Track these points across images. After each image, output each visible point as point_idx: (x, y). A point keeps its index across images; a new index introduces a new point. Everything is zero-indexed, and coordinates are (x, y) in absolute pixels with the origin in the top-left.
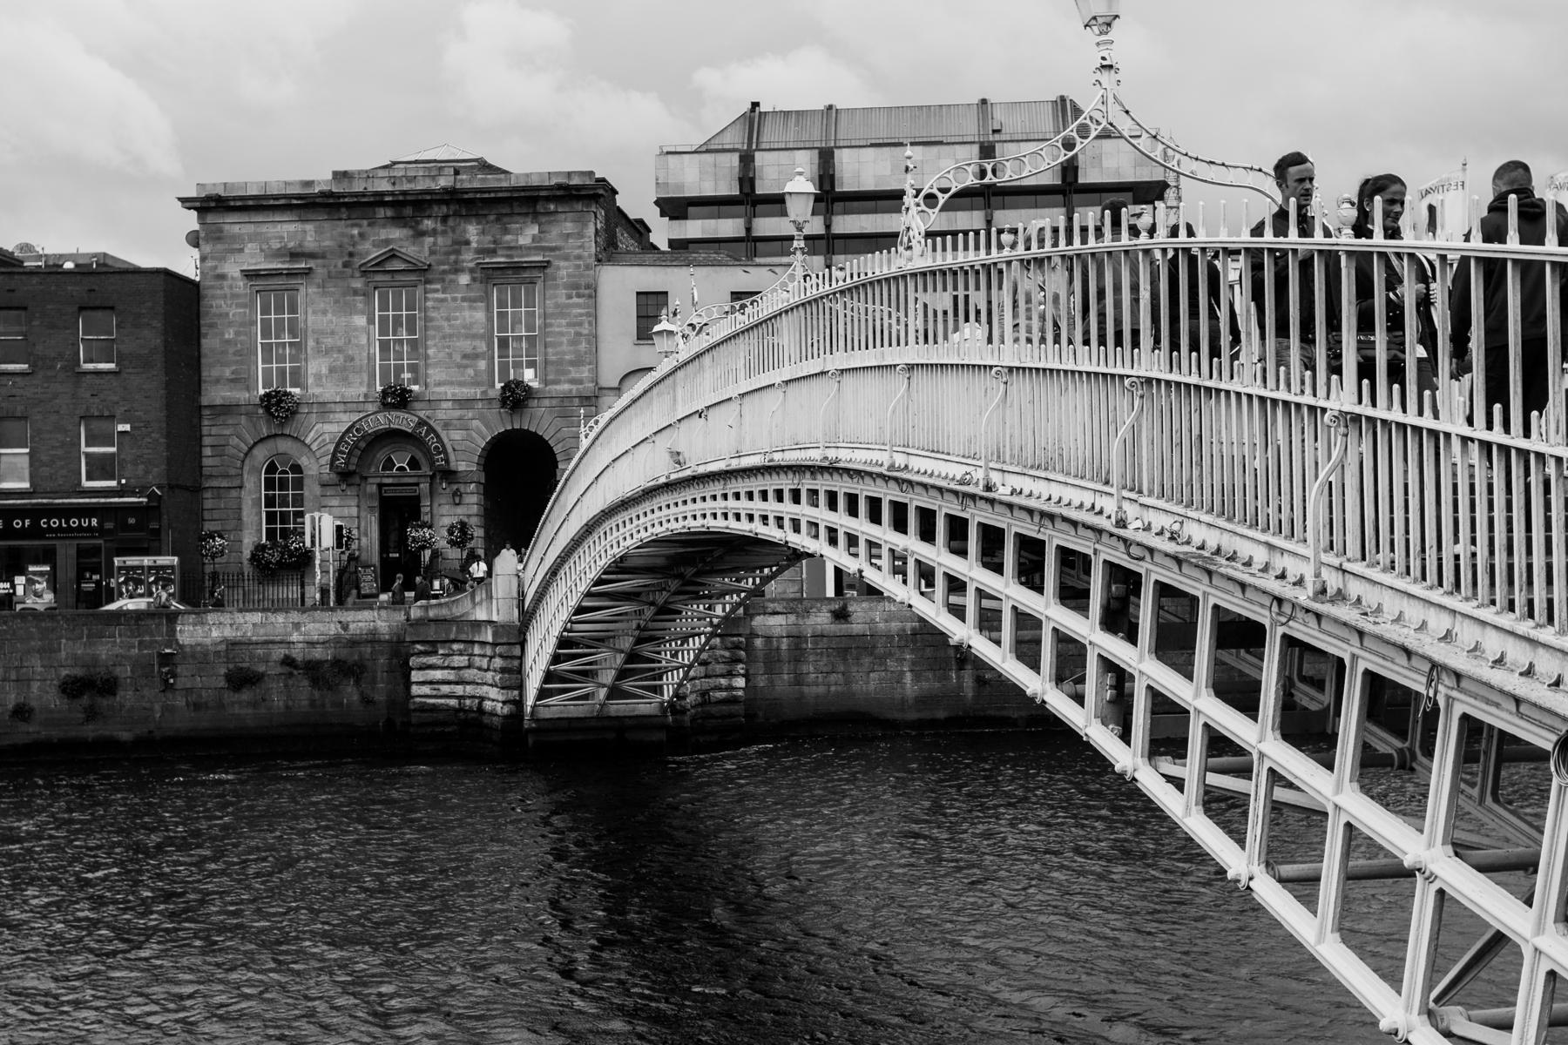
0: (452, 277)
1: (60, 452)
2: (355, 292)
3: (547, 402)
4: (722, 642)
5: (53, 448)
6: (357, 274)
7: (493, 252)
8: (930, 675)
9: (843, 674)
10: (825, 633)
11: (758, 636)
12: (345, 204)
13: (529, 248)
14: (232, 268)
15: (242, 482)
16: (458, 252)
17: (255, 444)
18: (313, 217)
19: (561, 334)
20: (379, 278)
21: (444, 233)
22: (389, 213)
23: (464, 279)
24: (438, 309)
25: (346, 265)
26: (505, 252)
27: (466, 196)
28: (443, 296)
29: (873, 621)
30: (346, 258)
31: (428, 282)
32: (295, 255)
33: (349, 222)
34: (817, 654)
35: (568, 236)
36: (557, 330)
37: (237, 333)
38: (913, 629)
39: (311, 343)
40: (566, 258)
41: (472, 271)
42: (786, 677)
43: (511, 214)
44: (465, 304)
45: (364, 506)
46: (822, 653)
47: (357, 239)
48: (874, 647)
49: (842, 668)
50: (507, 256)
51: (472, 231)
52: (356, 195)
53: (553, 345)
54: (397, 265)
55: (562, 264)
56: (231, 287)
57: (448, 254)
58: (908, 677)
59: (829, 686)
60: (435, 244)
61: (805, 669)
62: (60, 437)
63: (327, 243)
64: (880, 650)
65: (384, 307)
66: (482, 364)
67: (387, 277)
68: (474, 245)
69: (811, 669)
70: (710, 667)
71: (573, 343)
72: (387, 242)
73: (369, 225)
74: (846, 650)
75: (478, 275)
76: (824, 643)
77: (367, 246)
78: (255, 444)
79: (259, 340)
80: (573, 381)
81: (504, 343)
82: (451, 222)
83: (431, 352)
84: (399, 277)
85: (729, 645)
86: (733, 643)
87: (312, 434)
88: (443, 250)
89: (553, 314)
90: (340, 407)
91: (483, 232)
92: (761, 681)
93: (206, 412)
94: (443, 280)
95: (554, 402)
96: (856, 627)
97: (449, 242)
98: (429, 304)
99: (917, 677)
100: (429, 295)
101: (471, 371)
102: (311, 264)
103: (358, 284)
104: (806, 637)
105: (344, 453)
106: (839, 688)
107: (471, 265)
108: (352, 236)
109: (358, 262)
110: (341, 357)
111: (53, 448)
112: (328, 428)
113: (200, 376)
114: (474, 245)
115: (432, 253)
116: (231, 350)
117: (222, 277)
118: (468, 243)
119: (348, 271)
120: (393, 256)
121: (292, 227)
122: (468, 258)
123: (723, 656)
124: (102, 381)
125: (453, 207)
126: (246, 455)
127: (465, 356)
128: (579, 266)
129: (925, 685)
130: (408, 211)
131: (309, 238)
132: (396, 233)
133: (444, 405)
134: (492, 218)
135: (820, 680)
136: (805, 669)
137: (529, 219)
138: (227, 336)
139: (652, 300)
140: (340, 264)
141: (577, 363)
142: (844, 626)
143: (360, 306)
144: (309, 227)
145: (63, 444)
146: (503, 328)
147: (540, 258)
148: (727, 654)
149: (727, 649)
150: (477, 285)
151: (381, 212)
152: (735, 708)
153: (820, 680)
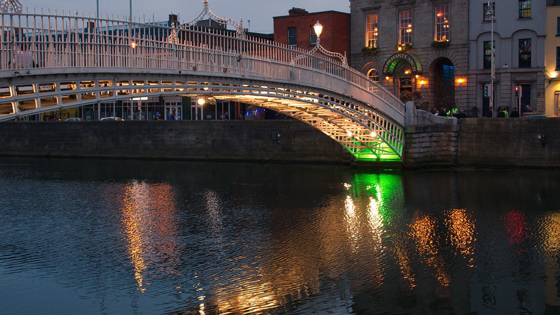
0: (422, 4)
3: (451, 47)
14: (358, 9)
20: (400, 7)
67: (403, 7)
86: (449, 134)
93: (352, 56)
100: (415, 12)
103: (394, 9)
105: (386, 68)
117: (356, 11)
133: (419, 50)
140: (389, 3)
148: (446, 138)
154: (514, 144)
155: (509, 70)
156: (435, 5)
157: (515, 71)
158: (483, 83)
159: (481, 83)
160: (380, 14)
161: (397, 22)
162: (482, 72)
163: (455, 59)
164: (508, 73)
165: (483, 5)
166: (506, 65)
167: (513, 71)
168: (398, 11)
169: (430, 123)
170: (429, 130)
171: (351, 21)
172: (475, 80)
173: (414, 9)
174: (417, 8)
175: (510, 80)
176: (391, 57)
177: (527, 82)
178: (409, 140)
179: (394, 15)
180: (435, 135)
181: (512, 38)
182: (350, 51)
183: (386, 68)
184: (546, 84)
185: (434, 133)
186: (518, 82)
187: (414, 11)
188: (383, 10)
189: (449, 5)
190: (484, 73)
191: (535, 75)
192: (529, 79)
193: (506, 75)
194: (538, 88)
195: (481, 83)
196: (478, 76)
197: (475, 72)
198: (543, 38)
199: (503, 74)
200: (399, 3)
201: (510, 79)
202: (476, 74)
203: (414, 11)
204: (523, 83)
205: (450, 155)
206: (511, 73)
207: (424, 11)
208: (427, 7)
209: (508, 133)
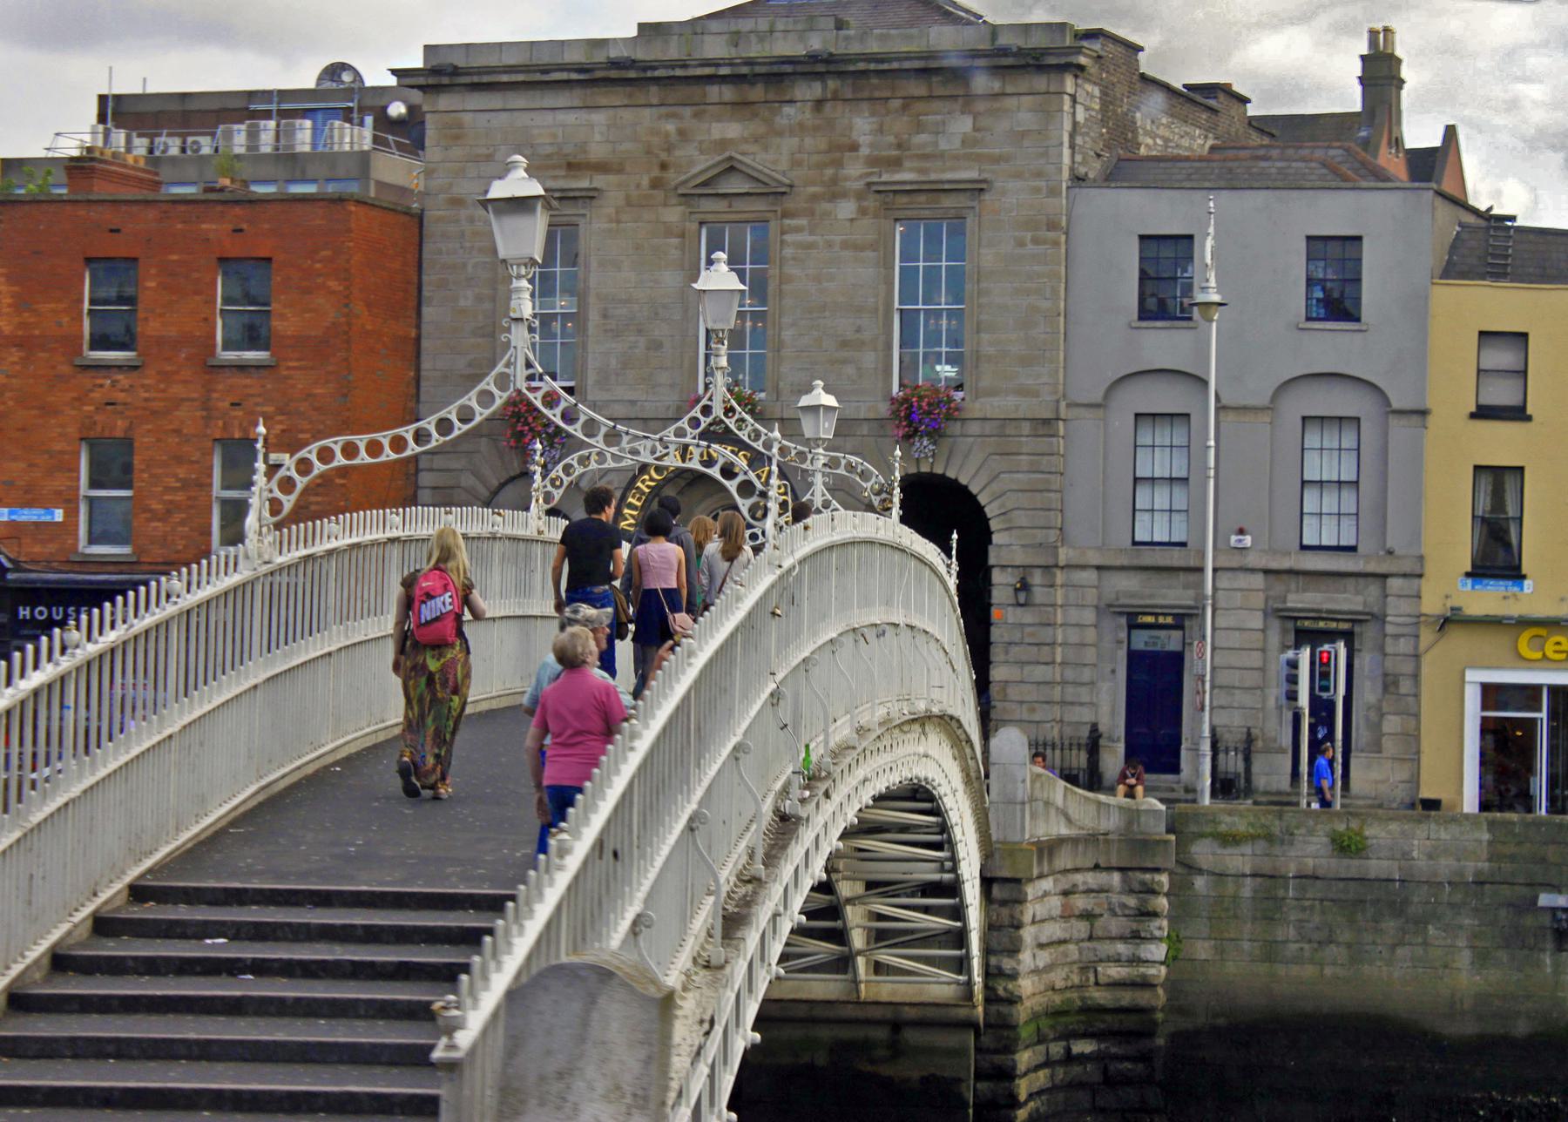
0: (826, 206)
1: (179, 497)
2: (669, 233)
3: (974, 428)
4: (1124, 881)
5: (168, 490)
6: (674, 201)
7: (896, 163)
8: (1503, 955)
9: (1349, 946)
10: (1320, 873)
11: (1200, 871)
12: (656, 80)
13: (956, 158)
16: (838, 164)
17: (503, 485)
18: (604, 101)
20: (708, 205)
21: (816, 129)
22: (728, 93)
23: (846, 209)
25: (656, 184)
26: (916, 164)
27: (852, 68)
29: (1406, 856)
30: (656, 173)
31: (785, 215)
32: (570, 166)
33: (663, 110)
34: (1304, 909)
35: (1024, 134)
37: (479, 299)
38: (1478, 873)
39: (594, 316)
40: (1018, 175)
41: (860, 196)
42: (1246, 945)
43: (931, 97)
44: (847, 254)
46: (1312, 908)
47: (674, 137)
48: (1406, 902)
49: (1346, 936)
50: (921, 171)
51: (862, 126)
52: (672, 65)
54: (735, 185)
55: (1011, 185)
57: (821, 166)
58: (1464, 959)
59: (1322, 965)
60: (800, 150)
61: (1280, 933)
62: (182, 472)
63: (627, 146)
64: (1412, 910)
66: (869, 359)
67: (721, 205)
68: (865, 151)
69: (1292, 932)
70: (1099, 923)
72: (723, 144)
73: (696, 115)
74: (1360, 902)
75: (871, 202)
76: (1315, 890)
77: (690, 151)
78: (503, 485)
80: (1023, 392)
81: (908, 318)
82: (828, 106)
83: (787, 335)
84: (739, 205)
85: (1136, 887)
86: (1143, 883)
88: (815, 158)
91: (881, 130)
92: (1202, 950)
94: (812, 213)
95: (988, 428)
96: (1376, 867)
97: (823, 146)
98: (788, 252)
99: (1482, 959)
100: (788, 238)
101: (850, 370)
102: (599, 181)
103: (673, 215)
104: (1285, 878)
105: (634, 508)
106: (1340, 971)
107: (859, 185)
108: (667, 135)
109: (673, 177)
111: (168, 490)
113: (418, 370)
114: (865, 151)
115: (796, 163)
118: (854, 147)
119: (659, 194)
120: (731, 169)
121: (570, 118)
122: (854, 171)
123: (1124, 906)
124: (248, 381)
125: (832, 84)
127: (844, 344)
128: (1037, 190)
129: (1494, 975)
130: (757, 93)
131: (598, 137)
132: (732, 130)
134: (896, 104)
135: (1307, 954)
136: (1280, 933)
137: (957, 106)
138: (462, 303)
139: (1167, 251)
140: (645, 182)
141: (1026, 361)
142: (1356, 862)
143: (675, 254)
144: (599, 118)
145: (186, 485)
146: (908, 295)
147: (973, 175)
148: (1132, 901)
149: (1132, 891)
150: (866, 222)
151: (713, 92)
152: (1142, 998)
153: (1307, 954)
154: (1431, 930)
155: (1253, 560)
157: (1286, 564)
158: (1129, 614)
159: (1121, 614)
162: (1125, 562)
164: (1253, 570)
166: (1241, 532)
167: (1274, 565)
168: (695, 226)
169: (1064, 831)
170: (1064, 860)
171: (428, 248)
172: (1091, 596)
173: (787, 222)
174: (803, 222)
175: (1262, 606)
177: (1337, 620)
178: (1005, 912)
180: (1085, 883)
181: (1270, 408)
182: (418, 401)
184: (1427, 636)
185: (1079, 878)
186: (1296, 619)
188: (611, 211)
190: (1136, 562)
191: (1373, 589)
192: (1345, 607)
193: (1243, 581)
194: (1389, 649)
195: (1121, 614)
196: (1106, 575)
197: (1094, 558)
198: (1415, 419)
199: (1229, 574)
200: (705, 184)
201: (1258, 600)
202: (1099, 568)
204: (1322, 624)
205: (1145, 984)
206: (1267, 572)
207: (838, 239)
208: (852, 220)
209: (1402, 881)
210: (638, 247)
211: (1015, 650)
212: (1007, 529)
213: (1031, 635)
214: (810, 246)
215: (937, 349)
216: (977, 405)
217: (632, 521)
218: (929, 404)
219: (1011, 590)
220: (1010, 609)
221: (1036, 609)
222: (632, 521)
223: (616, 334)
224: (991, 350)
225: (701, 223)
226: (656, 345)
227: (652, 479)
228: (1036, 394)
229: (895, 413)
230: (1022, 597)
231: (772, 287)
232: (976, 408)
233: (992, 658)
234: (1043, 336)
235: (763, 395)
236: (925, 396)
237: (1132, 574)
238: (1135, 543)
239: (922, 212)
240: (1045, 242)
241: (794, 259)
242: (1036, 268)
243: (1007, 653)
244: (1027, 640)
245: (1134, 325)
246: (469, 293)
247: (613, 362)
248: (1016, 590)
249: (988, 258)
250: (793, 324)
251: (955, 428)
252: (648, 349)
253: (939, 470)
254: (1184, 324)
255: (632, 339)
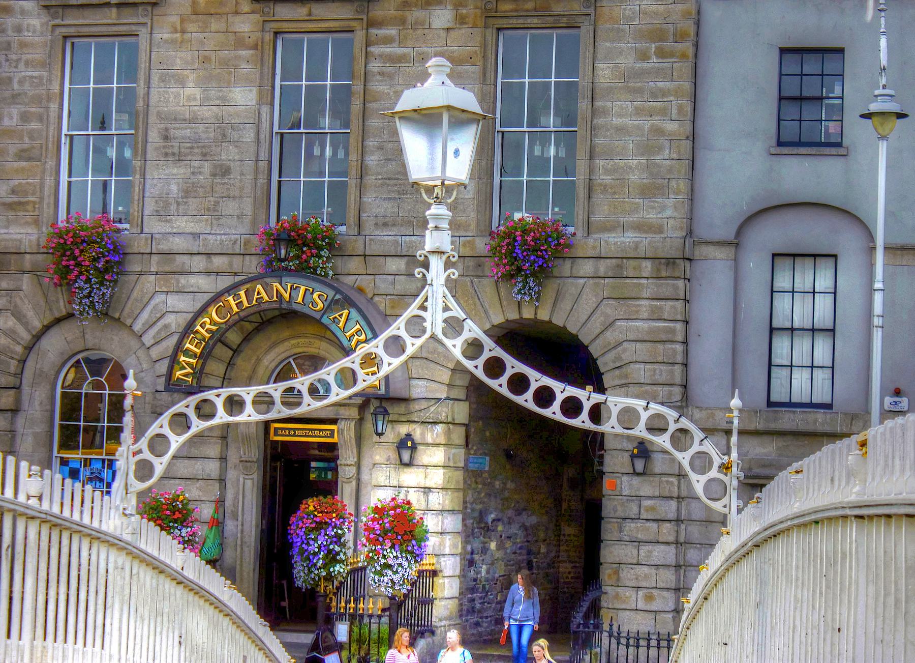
2: (240, 43)
3: (587, 268)
15: (18, 400)
17: (47, 328)
19: (621, 130)
24: (391, 76)
28: (400, 51)
36: (616, 121)
37: (25, 117)
39: (154, 136)
45: (233, 457)
53: (610, 154)
56: (18, 29)
65: (291, 73)
71: (647, 149)
78: (47, 328)
79: (65, 131)
80: (640, 227)
87: (145, 316)
89: (610, 90)
90: (199, 263)
94: (403, 22)
95: (603, 267)
100: (375, 50)
105: (194, 356)
110: (207, 166)
112: (174, 302)
116: (12, 149)
126: (29, 349)
138: (6, 122)
139: (811, 65)
141: (649, 191)
143: (246, 68)
150: (465, 31)
156: (503, 23)
160: (157, 36)
161: (260, 95)
163: (611, 336)
165: (778, 51)
168: (268, 37)
173: (374, 31)
174: (392, 32)
176: (229, 290)
179: (243, 53)
183: (187, 353)
187: (368, 44)
188: (175, 19)
189: (586, 29)
190: (773, 426)
203: (368, 44)
208: (448, 29)
210: (206, 60)
211: (630, 526)
212: (621, 386)
213: (652, 509)
214: (401, 59)
215: (547, 179)
216: (590, 241)
217: (189, 370)
218: (535, 239)
219: (627, 455)
220: (625, 478)
221: (657, 479)
222: (189, 370)
223: (179, 158)
224: (607, 179)
225: (276, 34)
226: (225, 171)
227: (213, 322)
228: (660, 230)
229: (494, 251)
230: (640, 465)
231: (356, 106)
232: (586, 245)
233: (604, 535)
234: (668, 162)
235: (343, 229)
236: (531, 230)
237: (766, 439)
238: (770, 404)
239: (529, 20)
240: (672, 55)
241: (382, 74)
242: (660, 84)
243: (621, 530)
244: (644, 516)
245: (773, 151)
246: (15, 112)
247: (174, 188)
248: (633, 457)
249: (605, 73)
250: (380, 148)
251: (566, 267)
252: (214, 175)
253: (544, 315)
254: (834, 151)
255: (196, 164)
